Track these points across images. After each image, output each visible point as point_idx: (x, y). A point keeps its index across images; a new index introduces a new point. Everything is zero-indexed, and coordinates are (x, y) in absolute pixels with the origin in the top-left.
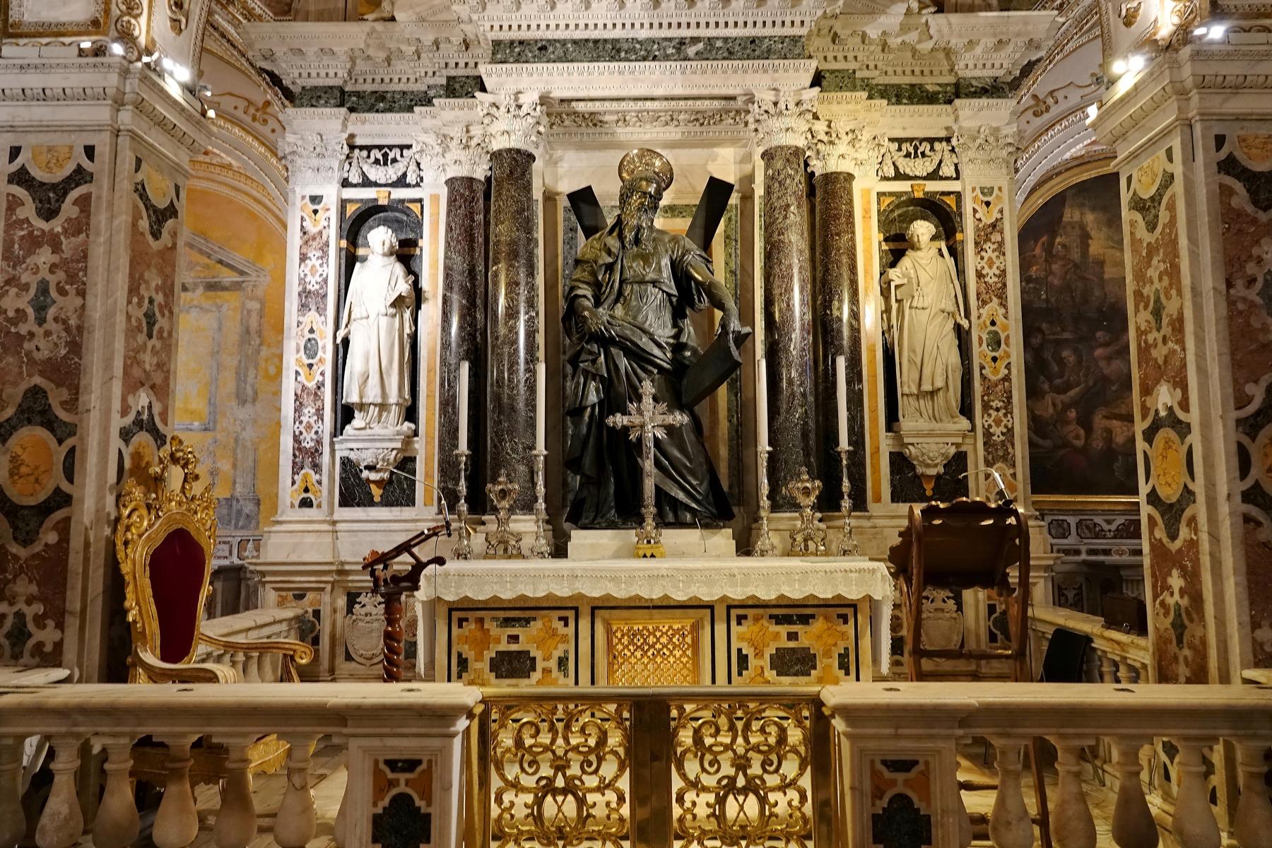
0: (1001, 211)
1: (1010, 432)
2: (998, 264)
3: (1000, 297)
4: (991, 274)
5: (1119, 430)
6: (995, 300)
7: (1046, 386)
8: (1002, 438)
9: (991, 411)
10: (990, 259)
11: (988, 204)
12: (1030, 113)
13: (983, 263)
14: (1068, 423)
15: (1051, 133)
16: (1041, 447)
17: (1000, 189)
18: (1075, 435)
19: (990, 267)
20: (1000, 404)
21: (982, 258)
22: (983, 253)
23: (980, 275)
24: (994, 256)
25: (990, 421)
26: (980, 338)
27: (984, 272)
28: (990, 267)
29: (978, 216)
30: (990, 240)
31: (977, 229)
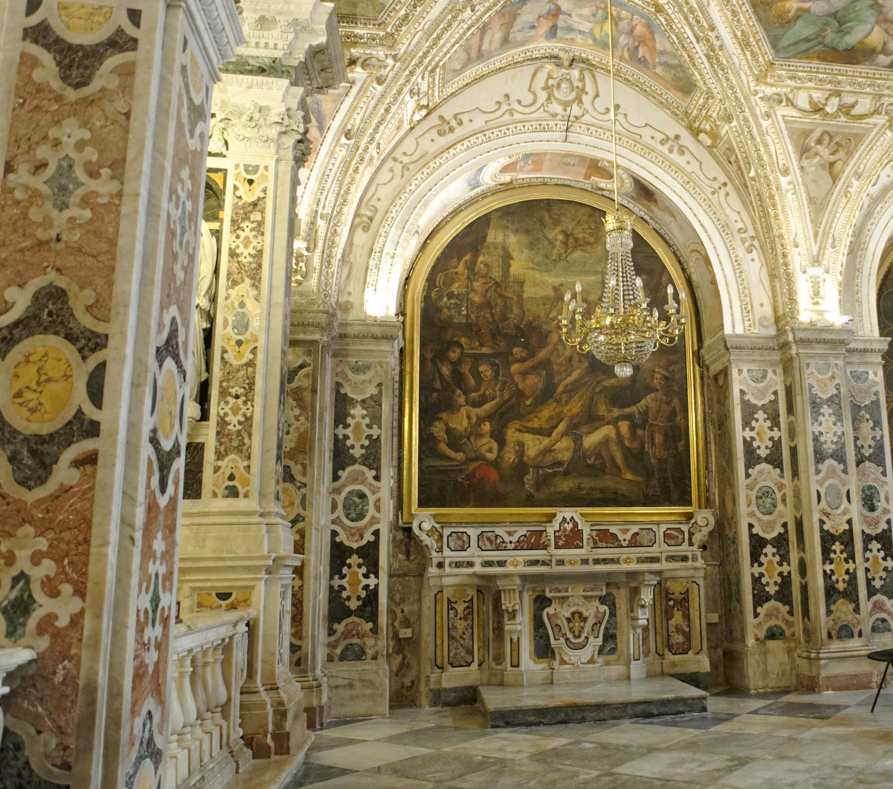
0: (265, 191)
1: (248, 421)
2: (254, 243)
3: (253, 278)
4: (246, 253)
5: (531, 444)
6: (248, 281)
7: (462, 400)
8: (239, 427)
9: (229, 399)
10: (247, 238)
11: (251, 182)
12: (434, 131)
13: (238, 242)
14: (480, 435)
15: (452, 151)
16: (454, 460)
17: (266, 168)
18: (487, 447)
19: (246, 247)
20: (241, 391)
21: (238, 237)
22: (240, 232)
23: (233, 254)
24: (251, 235)
25: (227, 409)
26: (226, 320)
27: (238, 251)
28: (246, 247)
29: (238, 193)
30: (249, 219)
31: (235, 206)
